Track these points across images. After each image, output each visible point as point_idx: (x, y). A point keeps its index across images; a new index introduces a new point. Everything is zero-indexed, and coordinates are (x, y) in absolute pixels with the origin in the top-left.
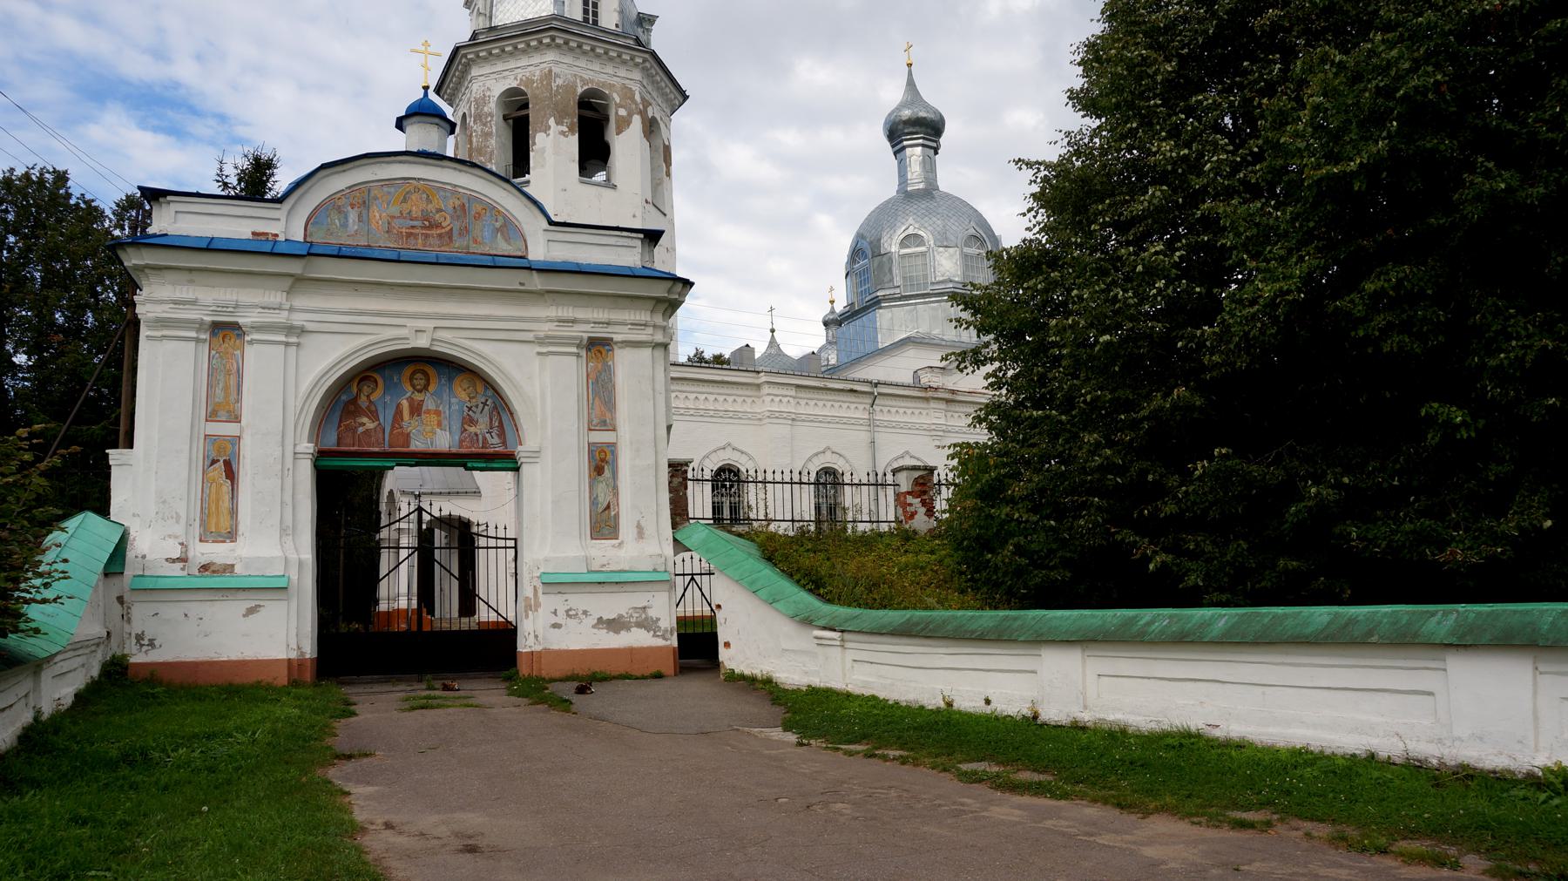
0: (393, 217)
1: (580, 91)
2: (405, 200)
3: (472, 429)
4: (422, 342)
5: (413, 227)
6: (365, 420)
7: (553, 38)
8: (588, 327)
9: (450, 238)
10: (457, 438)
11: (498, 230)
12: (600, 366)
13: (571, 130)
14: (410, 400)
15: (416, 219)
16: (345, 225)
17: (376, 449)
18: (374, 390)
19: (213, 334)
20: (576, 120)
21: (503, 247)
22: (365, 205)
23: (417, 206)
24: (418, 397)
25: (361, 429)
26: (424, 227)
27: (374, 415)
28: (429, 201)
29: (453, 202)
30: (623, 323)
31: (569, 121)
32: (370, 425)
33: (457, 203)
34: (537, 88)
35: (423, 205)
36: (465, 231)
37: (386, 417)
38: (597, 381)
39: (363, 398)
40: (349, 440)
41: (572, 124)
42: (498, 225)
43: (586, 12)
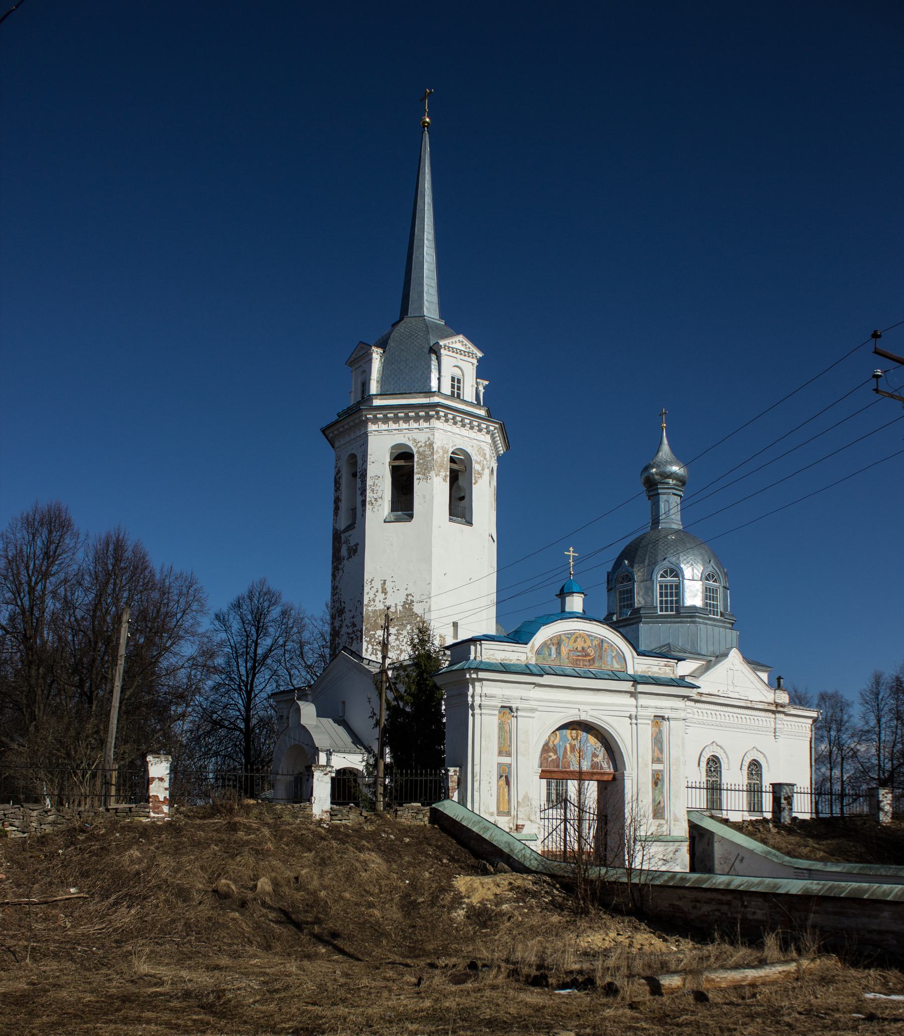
0: (570, 651)
1: (451, 450)
2: (575, 641)
3: (595, 760)
4: (584, 717)
5: (578, 656)
6: (551, 754)
7: (437, 413)
8: (653, 710)
9: (594, 662)
10: (590, 764)
11: (613, 657)
12: (657, 730)
13: (444, 480)
14: (570, 744)
15: (579, 652)
16: (550, 655)
17: (556, 769)
18: (556, 739)
19: (500, 712)
20: (448, 473)
21: (616, 666)
22: (559, 644)
23: (580, 644)
24: (573, 742)
25: (550, 759)
26: (583, 656)
27: (555, 752)
28: (585, 642)
29: (596, 642)
30: (665, 705)
31: (444, 474)
32: (554, 757)
33: (597, 643)
34: (421, 446)
35: (582, 644)
36: (601, 657)
37: (561, 752)
38: (655, 738)
39: (551, 743)
40: (545, 765)
41: (446, 476)
42: (614, 654)
43: (453, 386)
